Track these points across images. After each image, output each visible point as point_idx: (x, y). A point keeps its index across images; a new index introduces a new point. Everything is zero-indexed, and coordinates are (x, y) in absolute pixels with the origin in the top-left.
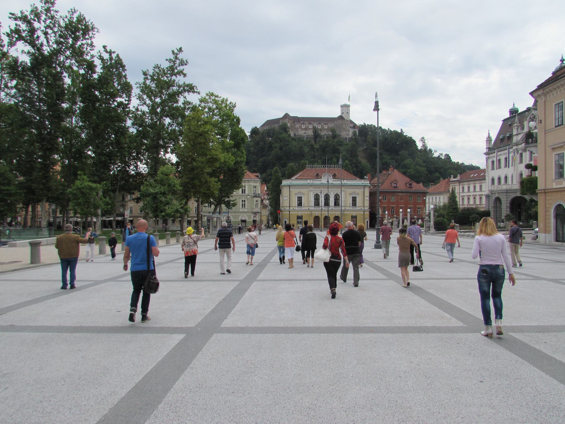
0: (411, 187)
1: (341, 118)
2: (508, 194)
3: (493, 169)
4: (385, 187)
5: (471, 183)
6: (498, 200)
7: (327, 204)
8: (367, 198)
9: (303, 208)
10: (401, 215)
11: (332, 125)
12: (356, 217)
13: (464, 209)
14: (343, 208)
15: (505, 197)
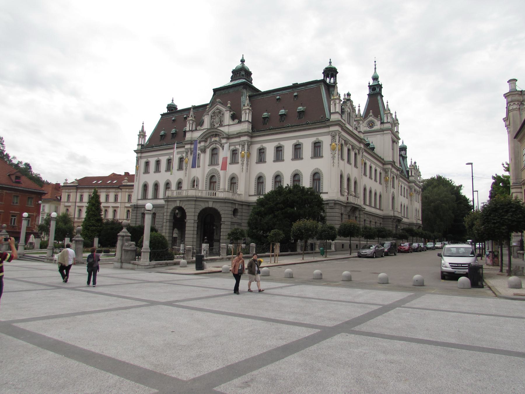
0: (19, 183)
2: (197, 203)
3: (146, 171)
10: (24, 223)
13: (108, 223)
15: (193, 206)
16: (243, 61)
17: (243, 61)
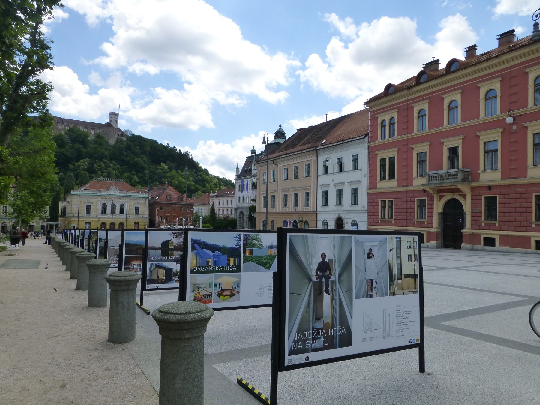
1: (109, 125)
4: (162, 199)
5: (225, 198)
6: (242, 213)
7: (113, 212)
8: (147, 208)
9: (91, 215)
11: (100, 131)
12: (138, 223)
14: (128, 216)
16: (280, 126)
17: (280, 126)
